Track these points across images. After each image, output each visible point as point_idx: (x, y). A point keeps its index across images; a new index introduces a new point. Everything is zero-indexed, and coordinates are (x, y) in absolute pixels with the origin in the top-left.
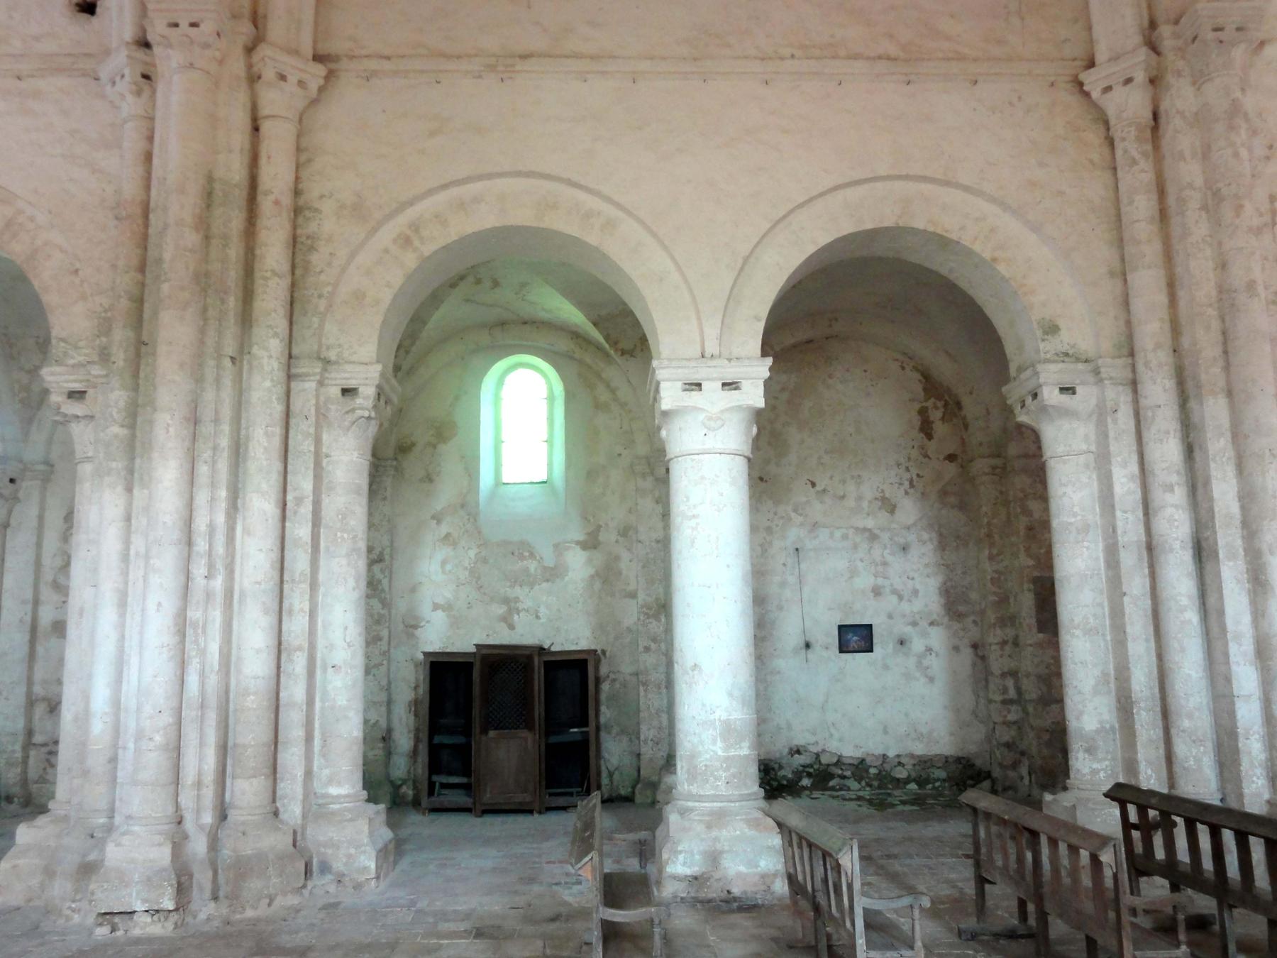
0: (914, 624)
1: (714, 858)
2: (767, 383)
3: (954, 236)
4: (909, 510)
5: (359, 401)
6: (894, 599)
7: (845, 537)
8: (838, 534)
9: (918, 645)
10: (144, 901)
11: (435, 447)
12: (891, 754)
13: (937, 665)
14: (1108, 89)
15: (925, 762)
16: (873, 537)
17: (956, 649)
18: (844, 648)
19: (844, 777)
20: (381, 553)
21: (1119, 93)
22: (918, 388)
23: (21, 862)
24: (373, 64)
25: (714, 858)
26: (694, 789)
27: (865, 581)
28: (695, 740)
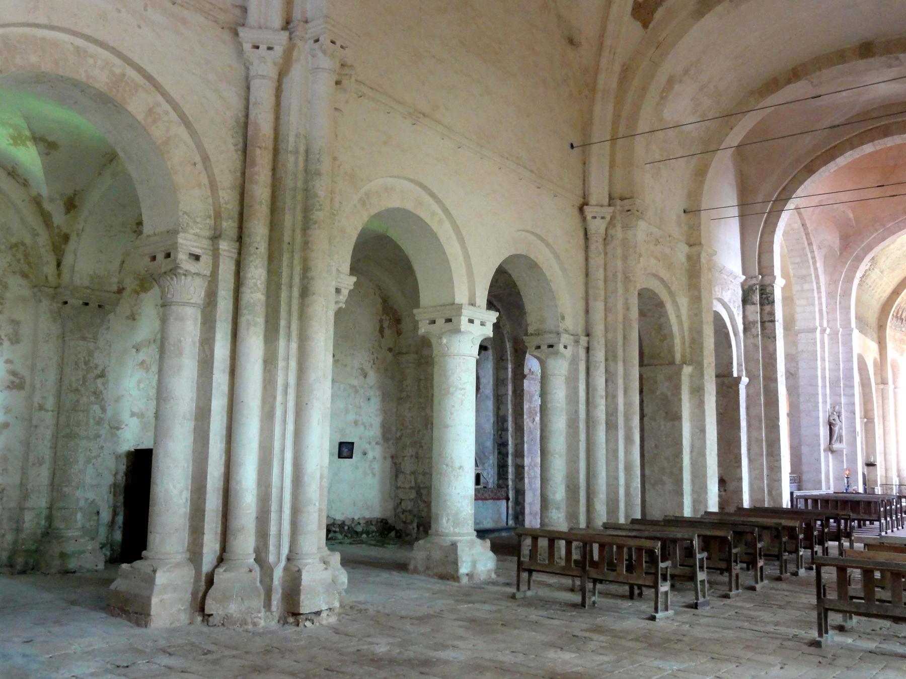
0: (370, 443)
1: (474, 564)
2: (494, 325)
3: (541, 266)
4: (373, 377)
5: (341, 297)
6: (362, 428)
7: (345, 390)
8: (342, 387)
9: (370, 455)
10: (327, 603)
11: (138, 293)
12: (356, 518)
13: (377, 466)
14: (594, 218)
15: (369, 522)
16: (356, 392)
17: (385, 458)
18: (340, 456)
19: (335, 532)
20: (103, 370)
21: (598, 221)
22: (379, 307)
23: (165, 597)
24: (365, 90)
25: (474, 564)
26: (457, 530)
27: (351, 417)
28: (459, 505)
